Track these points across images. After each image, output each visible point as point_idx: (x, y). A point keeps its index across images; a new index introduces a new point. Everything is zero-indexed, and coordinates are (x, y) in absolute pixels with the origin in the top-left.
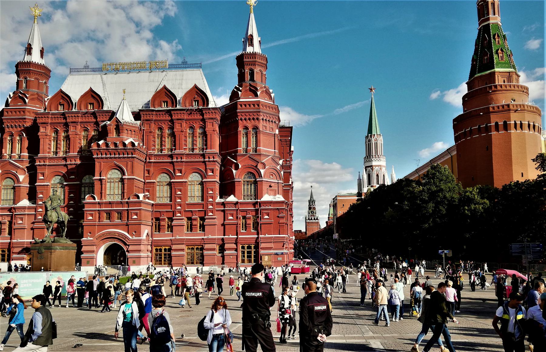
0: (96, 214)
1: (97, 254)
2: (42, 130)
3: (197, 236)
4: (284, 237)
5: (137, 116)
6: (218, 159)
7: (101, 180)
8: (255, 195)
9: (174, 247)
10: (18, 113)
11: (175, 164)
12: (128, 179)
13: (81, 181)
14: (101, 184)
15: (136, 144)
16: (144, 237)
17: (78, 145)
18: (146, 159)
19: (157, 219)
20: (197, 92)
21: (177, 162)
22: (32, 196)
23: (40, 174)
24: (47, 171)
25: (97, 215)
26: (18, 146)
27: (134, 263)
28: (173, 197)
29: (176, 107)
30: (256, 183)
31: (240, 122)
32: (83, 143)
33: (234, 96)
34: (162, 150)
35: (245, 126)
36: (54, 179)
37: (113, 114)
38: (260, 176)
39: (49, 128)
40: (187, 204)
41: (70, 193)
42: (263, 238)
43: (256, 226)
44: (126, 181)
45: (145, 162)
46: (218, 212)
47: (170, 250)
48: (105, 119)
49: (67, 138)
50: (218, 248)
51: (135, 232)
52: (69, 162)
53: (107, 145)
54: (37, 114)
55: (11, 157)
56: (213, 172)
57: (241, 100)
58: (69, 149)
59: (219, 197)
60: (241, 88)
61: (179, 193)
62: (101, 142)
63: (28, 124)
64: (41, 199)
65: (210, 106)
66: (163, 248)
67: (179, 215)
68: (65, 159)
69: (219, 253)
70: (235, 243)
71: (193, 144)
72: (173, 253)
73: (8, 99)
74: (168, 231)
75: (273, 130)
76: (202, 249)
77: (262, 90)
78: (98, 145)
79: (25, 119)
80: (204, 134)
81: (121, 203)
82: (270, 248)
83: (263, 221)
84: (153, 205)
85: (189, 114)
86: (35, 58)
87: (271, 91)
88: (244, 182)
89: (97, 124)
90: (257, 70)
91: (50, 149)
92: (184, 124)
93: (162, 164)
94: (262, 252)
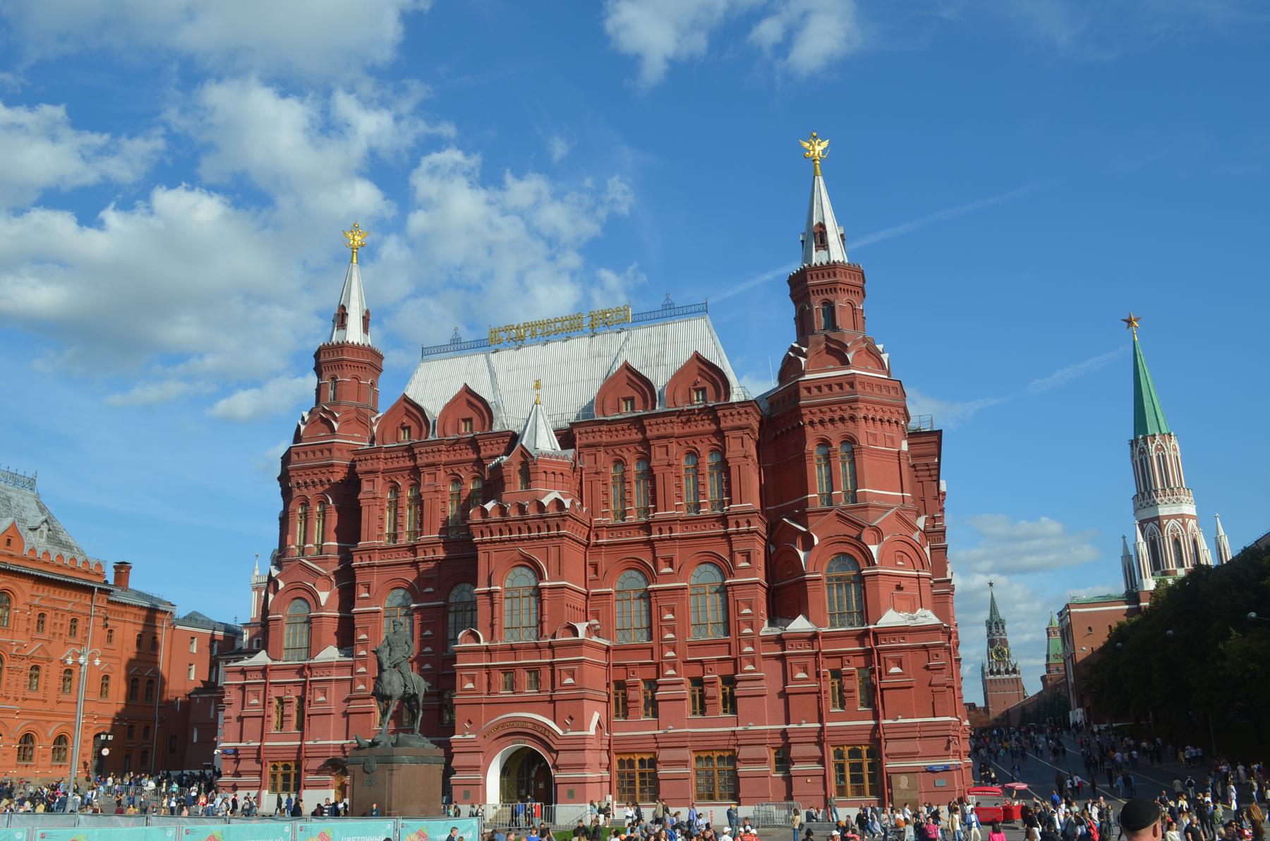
0: (481, 677)
1: (485, 775)
2: (366, 486)
3: (718, 726)
4: (947, 724)
5: (566, 437)
6: (758, 526)
7: (490, 593)
9: (663, 755)
10: (319, 454)
11: (657, 545)
12: (550, 588)
13: (447, 600)
14: (492, 605)
15: (567, 504)
16: (592, 731)
17: (441, 516)
18: (588, 538)
19: (621, 685)
20: (700, 369)
21: (661, 540)
22: (346, 638)
24: (376, 579)
25: (485, 676)
26: (317, 526)
27: (572, 797)
28: (655, 628)
29: (654, 408)
30: (860, 580)
31: (809, 429)
32: (451, 510)
33: (790, 368)
34: (624, 513)
35: (822, 440)
36: (390, 596)
37: (514, 438)
38: (870, 560)
39: (380, 481)
41: (424, 627)
42: (891, 726)
43: (872, 696)
44: (546, 593)
45: (587, 546)
46: (769, 662)
47: (653, 763)
48: (496, 452)
49: (418, 501)
50: (773, 757)
51: (571, 718)
52: (420, 557)
53: (503, 510)
54: (356, 452)
55: (303, 552)
56: (749, 560)
57: (807, 377)
58: (421, 525)
59: (766, 623)
60: (804, 350)
61: (670, 616)
62: (489, 506)
63: (338, 477)
64: (364, 643)
65: (734, 398)
67: (672, 672)
68: (413, 549)
69: (777, 769)
70: (816, 743)
71: (698, 494)
72: (662, 771)
73: (299, 427)
74: (647, 715)
75: (893, 442)
76: (733, 759)
77: (858, 347)
78: (484, 513)
79: (332, 465)
80: (724, 467)
81: (537, 647)
82: (912, 755)
83: (887, 681)
84: (608, 649)
85: (685, 423)
86: (354, 333)
87: (880, 347)
88: (829, 579)
89: (479, 463)
90: (841, 302)
91: (381, 528)
92: (674, 448)
93: (626, 548)
94: (890, 765)
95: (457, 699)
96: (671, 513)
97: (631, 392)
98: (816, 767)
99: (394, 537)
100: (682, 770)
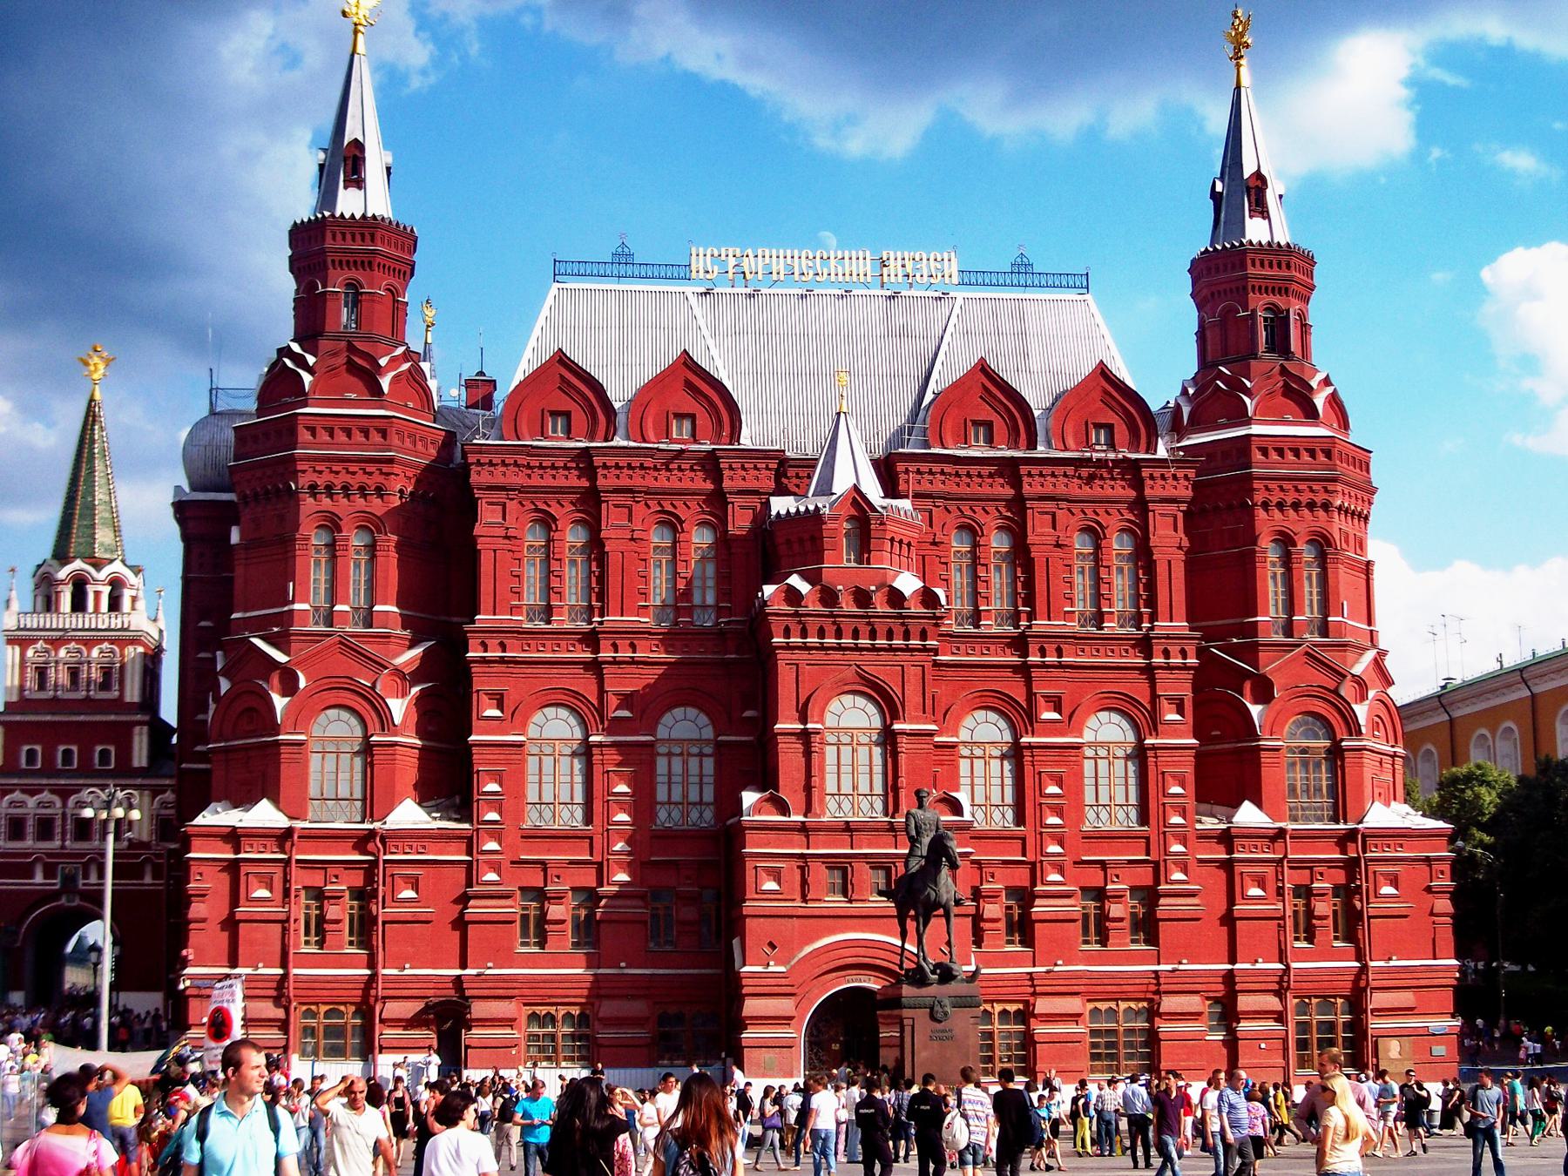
5: (887, 469)
8: (1335, 806)
9: (1042, 1006)
11: (1035, 673)
20: (1106, 392)
23: (485, 698)
26: (356, 577)
29: (1032, 445)
30: (1336, 754)
31: (1261, 514)
38: (1354, 728)
40: (1088, 837)
42: (1380, 970)
66: (998, 1008)
71: (1098, 597)
79: (390, 461)
83: (1375, 906)
93: (980, 672)
94: (1375, 1024)
95: (750, 906)
96: (1057, 625)
97: (986, 413)
98: (1271, 1025)
99: (548, 612)
100: (1071, 1028)
